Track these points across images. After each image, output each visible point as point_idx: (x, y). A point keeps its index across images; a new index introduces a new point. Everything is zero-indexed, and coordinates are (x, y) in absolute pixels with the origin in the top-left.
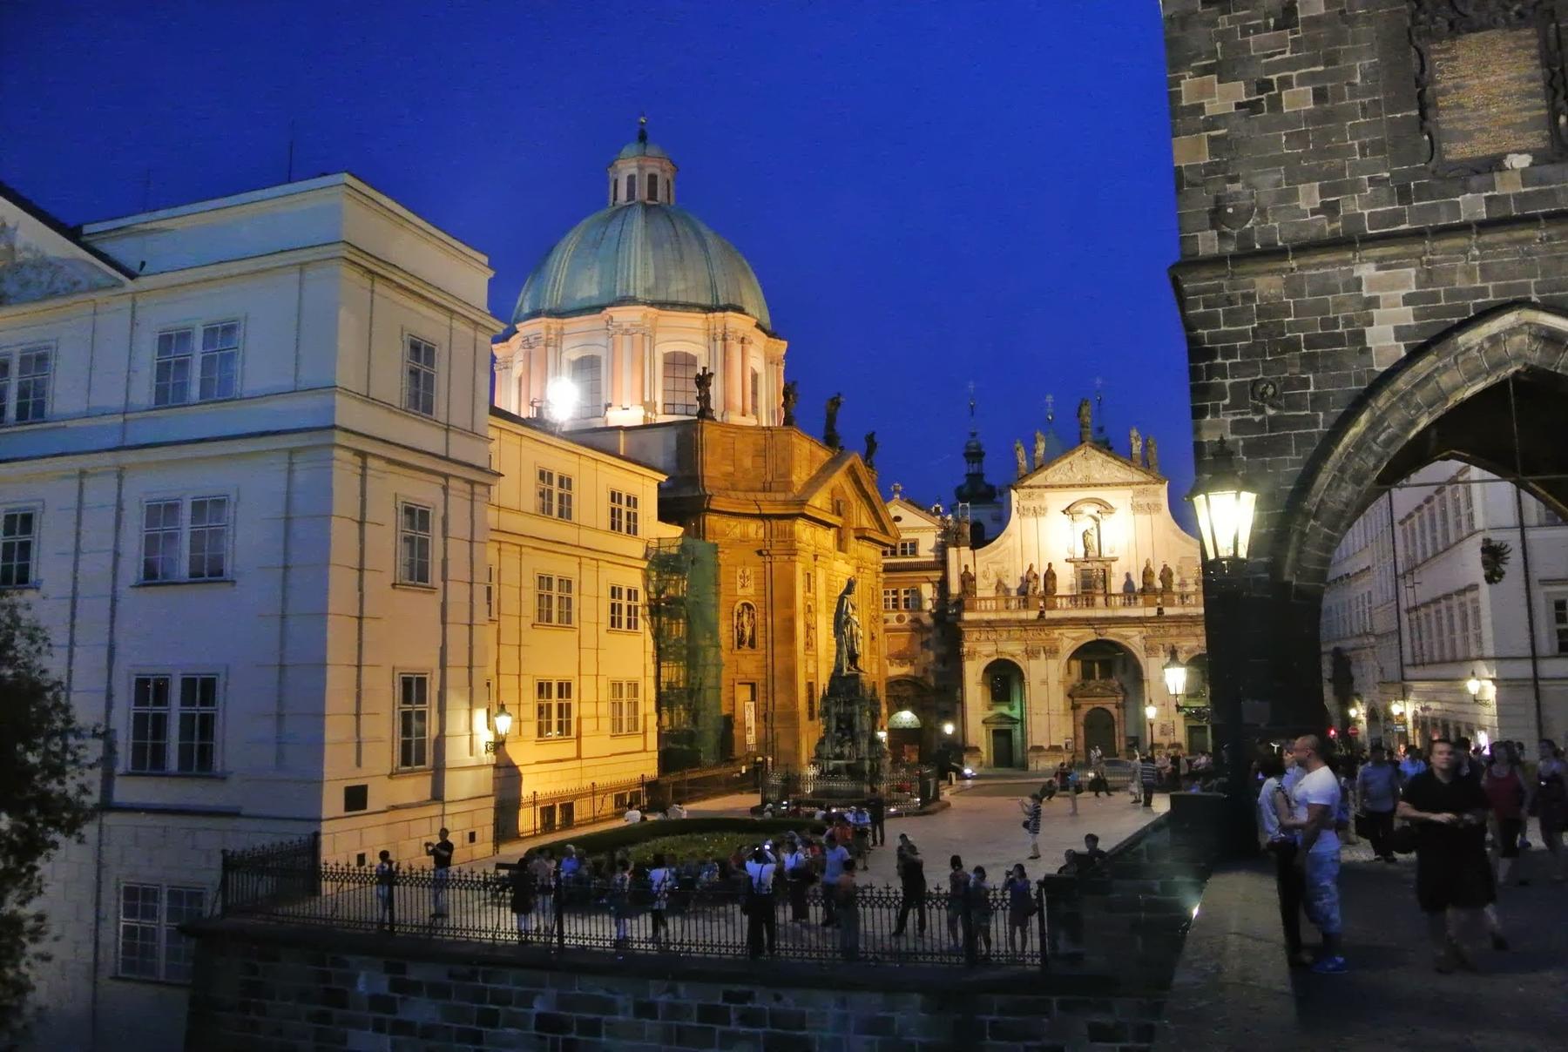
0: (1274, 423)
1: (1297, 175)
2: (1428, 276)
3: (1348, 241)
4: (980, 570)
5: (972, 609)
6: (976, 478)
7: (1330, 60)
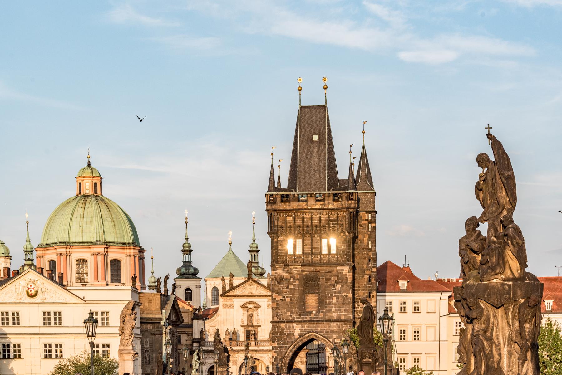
0: (282, 344)
2: (302, 327)
3: (292, 322)
4: (207, 329)
5: (204, 346)
7: (293, 295)
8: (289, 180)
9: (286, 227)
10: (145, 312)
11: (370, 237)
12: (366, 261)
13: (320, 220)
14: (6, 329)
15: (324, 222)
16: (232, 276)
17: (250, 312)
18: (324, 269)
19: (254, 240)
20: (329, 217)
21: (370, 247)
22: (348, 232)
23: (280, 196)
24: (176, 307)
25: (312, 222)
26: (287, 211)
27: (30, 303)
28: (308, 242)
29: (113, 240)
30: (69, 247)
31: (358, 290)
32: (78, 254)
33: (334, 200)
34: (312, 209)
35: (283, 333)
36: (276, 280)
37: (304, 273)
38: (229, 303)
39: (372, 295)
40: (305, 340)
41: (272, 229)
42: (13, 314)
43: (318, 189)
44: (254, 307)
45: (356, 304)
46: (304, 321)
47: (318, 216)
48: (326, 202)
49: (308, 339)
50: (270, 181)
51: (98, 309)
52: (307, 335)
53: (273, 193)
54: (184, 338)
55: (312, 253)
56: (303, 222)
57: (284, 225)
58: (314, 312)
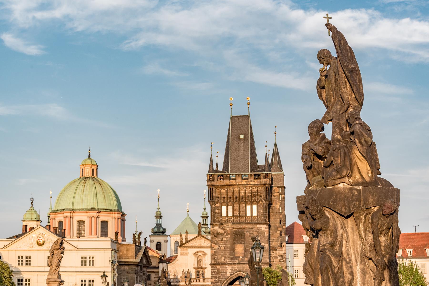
0: (218, 280)
1: (222, 256)
2: (232, 267)
3: (225, 264)
4: (169, 270)
6: (159, 225)
7: (226, 245)
8: (224, 165)
9: (221, 197)
10: (124, 258)
11: (281, 204)
12: (278, 221)
13: (245, 192)
14: (21, 268)
15: (248, 194)
16: (187, 233)
17: (199, 258)
18: (248, 226)
19: (205, 209)
20: (251, 190)
21: (281, 211)
22: (265, 201)
23: (217, 176)
24: (147, 254)
25: (239, 194)
26: (222, 186)
27: (38, 250)
28: (236, 207)
29: (103, 208)
30: (72, 212)
31: (273, 242)
32: (78, 217)
33: (255, 179)
34: (239, 185)
35: (218, 272)
36: (214, 234)
37: (234, 230)
38: (185, 252)
39: (282, 245)
40: (235, 277)
41: (211, 198)
42: (27, 257)
43: (244, 171)
44: (203, 255)
45: (271, 252)
46: (234, 264)
47: (244, 190)
48: (249, 180)
49: (237, 276)
50: (210, 165)
51: (87, 254)
52: (236, 274)
53: (212, 174)
54: (153, 276)
55: (239, 215)
56: (233, 194)
57: (219, 196)
58: (241, 257)
